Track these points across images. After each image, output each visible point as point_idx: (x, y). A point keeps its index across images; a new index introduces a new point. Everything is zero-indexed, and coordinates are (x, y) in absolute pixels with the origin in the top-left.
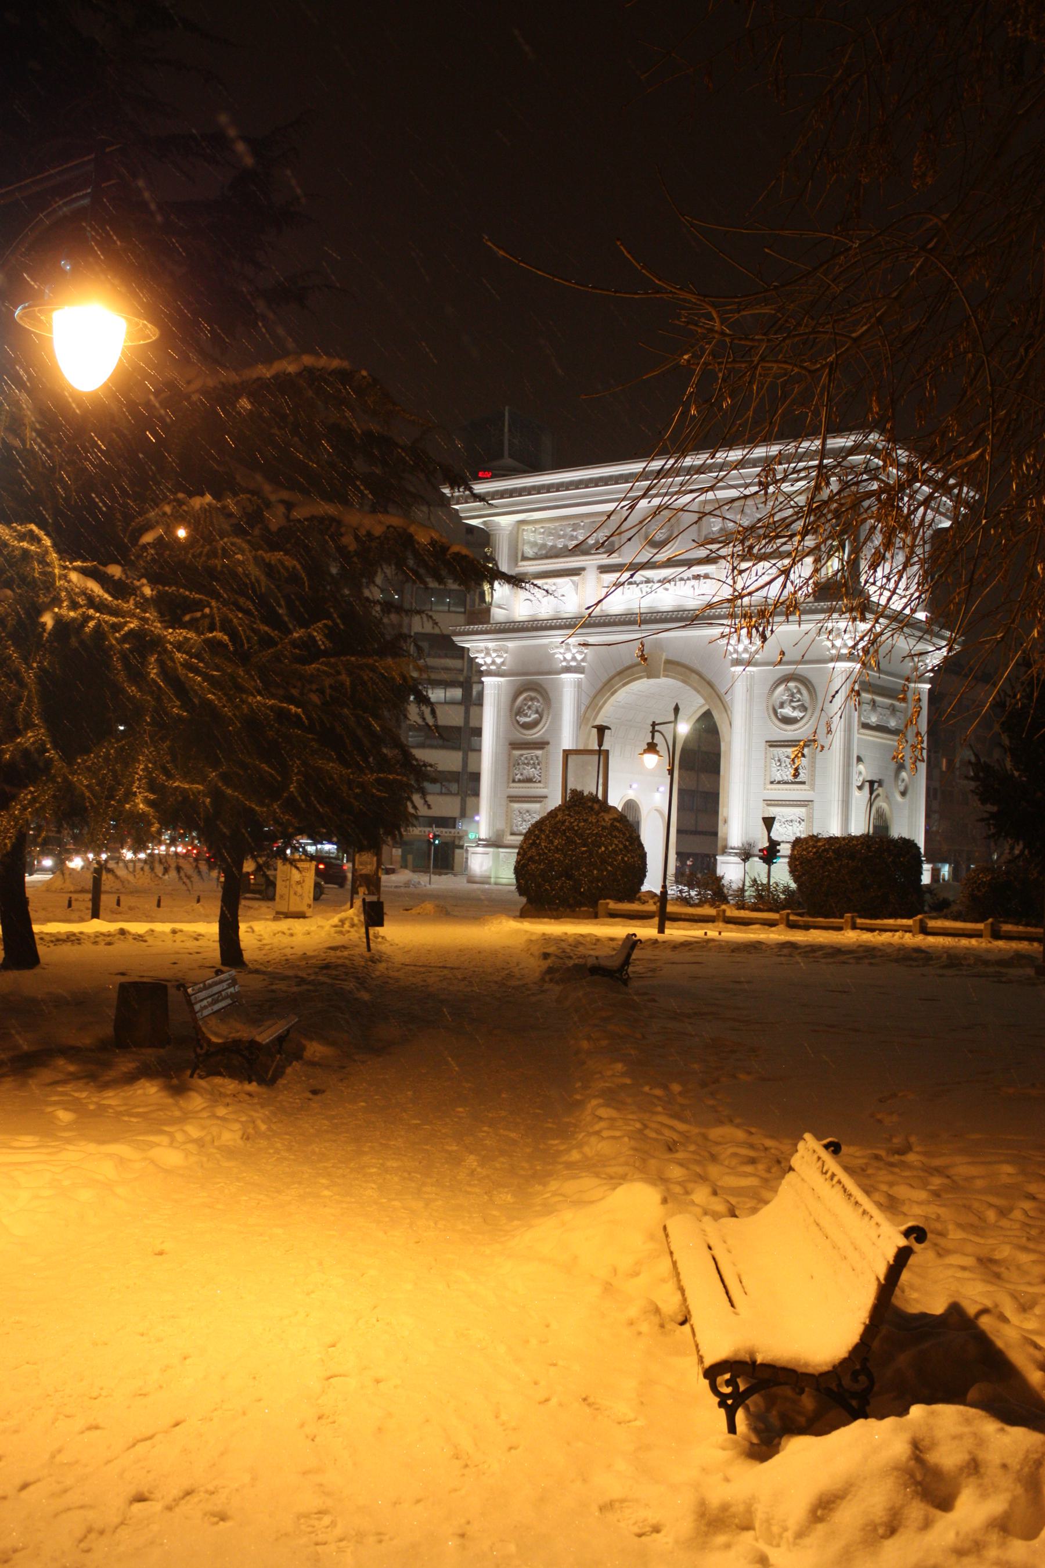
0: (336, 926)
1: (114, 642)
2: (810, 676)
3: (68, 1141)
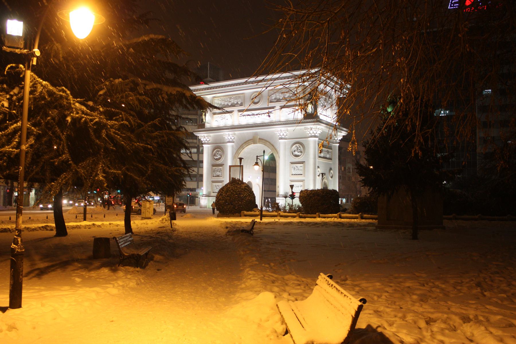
0: (161, 221)
1: (91, 125)
3: (80, 287)
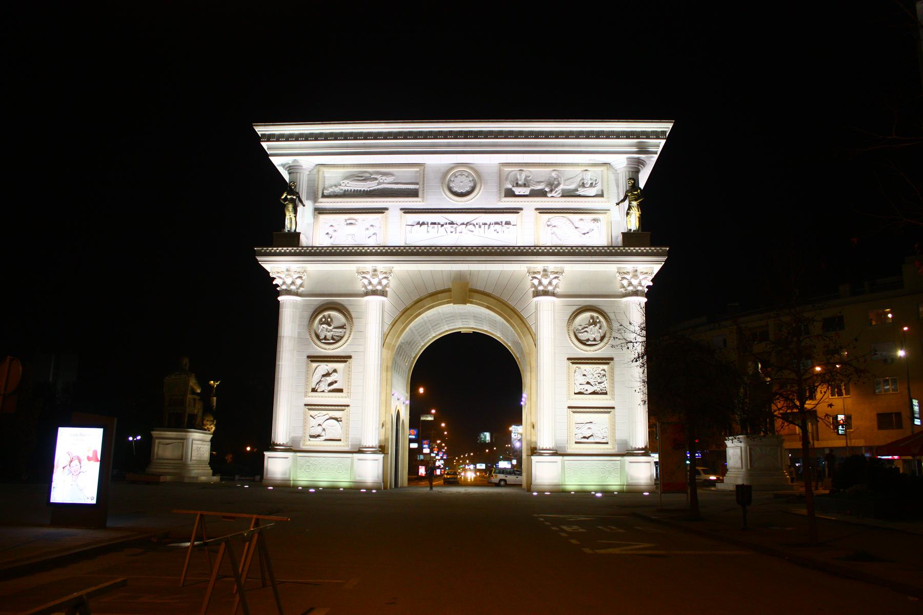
2: (605, 309)
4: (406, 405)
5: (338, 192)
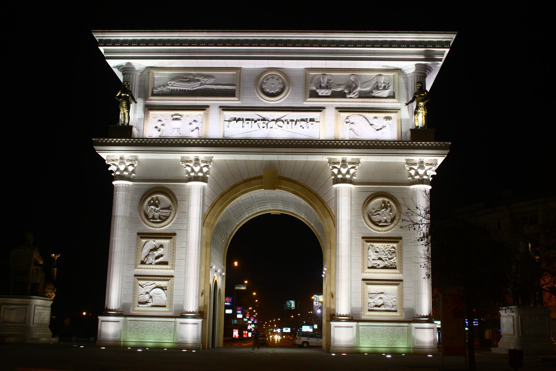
2: (394, 195)
4: (223, 276)
5: (166, 91)
